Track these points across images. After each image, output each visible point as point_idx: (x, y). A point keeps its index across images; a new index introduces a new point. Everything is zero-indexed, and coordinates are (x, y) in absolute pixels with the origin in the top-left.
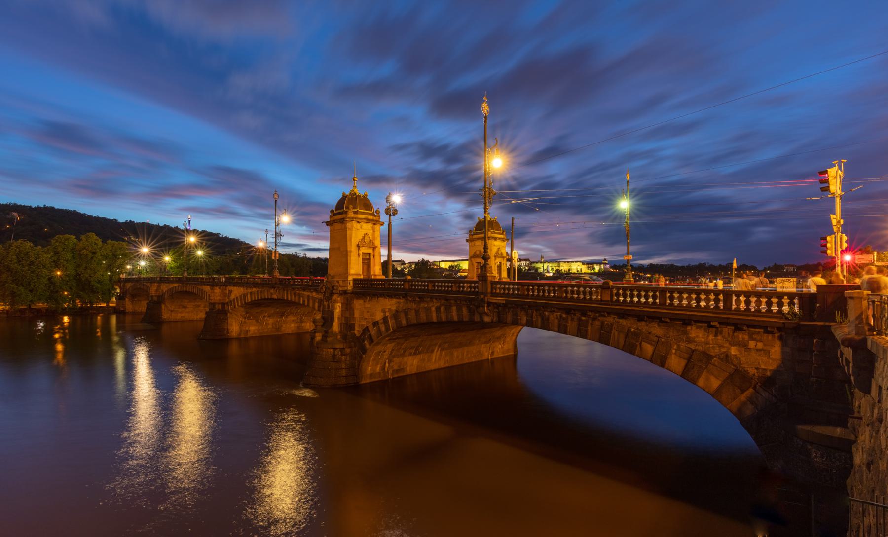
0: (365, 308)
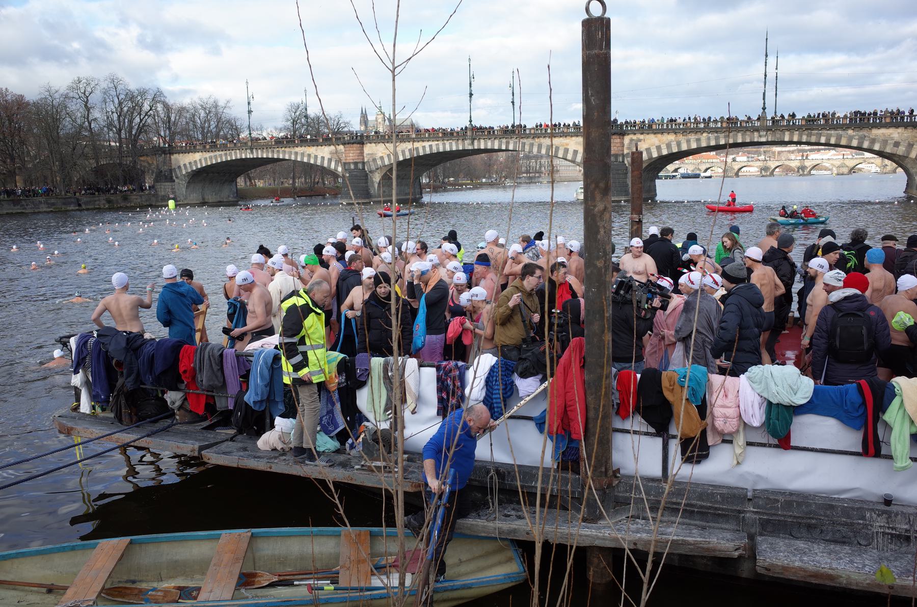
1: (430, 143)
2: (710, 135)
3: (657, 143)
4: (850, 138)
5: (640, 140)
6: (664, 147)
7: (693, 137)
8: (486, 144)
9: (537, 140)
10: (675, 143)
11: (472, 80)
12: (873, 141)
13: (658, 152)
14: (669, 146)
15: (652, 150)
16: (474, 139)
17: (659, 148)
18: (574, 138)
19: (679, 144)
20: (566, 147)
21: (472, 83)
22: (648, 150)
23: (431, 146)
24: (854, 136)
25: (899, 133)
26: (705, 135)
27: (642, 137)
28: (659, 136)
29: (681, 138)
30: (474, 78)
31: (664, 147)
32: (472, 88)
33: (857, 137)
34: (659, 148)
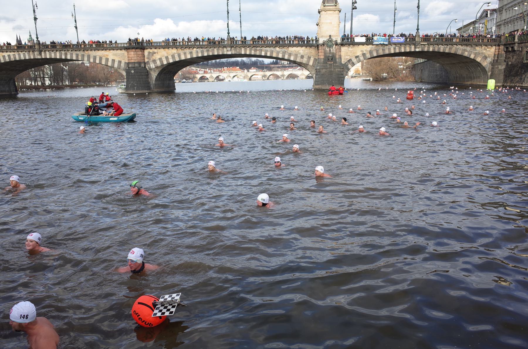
0: (349, 51)
1: (9, 53)
2: (198, 50)
3: (166, 55)
4: (278, 53)
5: (155, 53)
6: (170, 57)
7: (187, 51)
8: (50, 55)
9: (86, 52)
10: (177, 55)
11: (36, 7)
12: (290, 55)
13: (167, 61)
14: (173, 56)
15: (163, 60)
16: (41, 51)
17: (167, 58)
18: (111, 51)
19: (179, 55)
20: (107, 57)
21: (36, 10)
22: (160, 59)
23: (9, 56)
24: (279, 51)
25: (303, 50)
26: (195, 49)
27: (156, 50)
28: (167, 50)
29: (180, 51)
30: (37, 6)
31: (170, 57)
32: (36, 14)
33: (281, 52)
34: (167, 58)
